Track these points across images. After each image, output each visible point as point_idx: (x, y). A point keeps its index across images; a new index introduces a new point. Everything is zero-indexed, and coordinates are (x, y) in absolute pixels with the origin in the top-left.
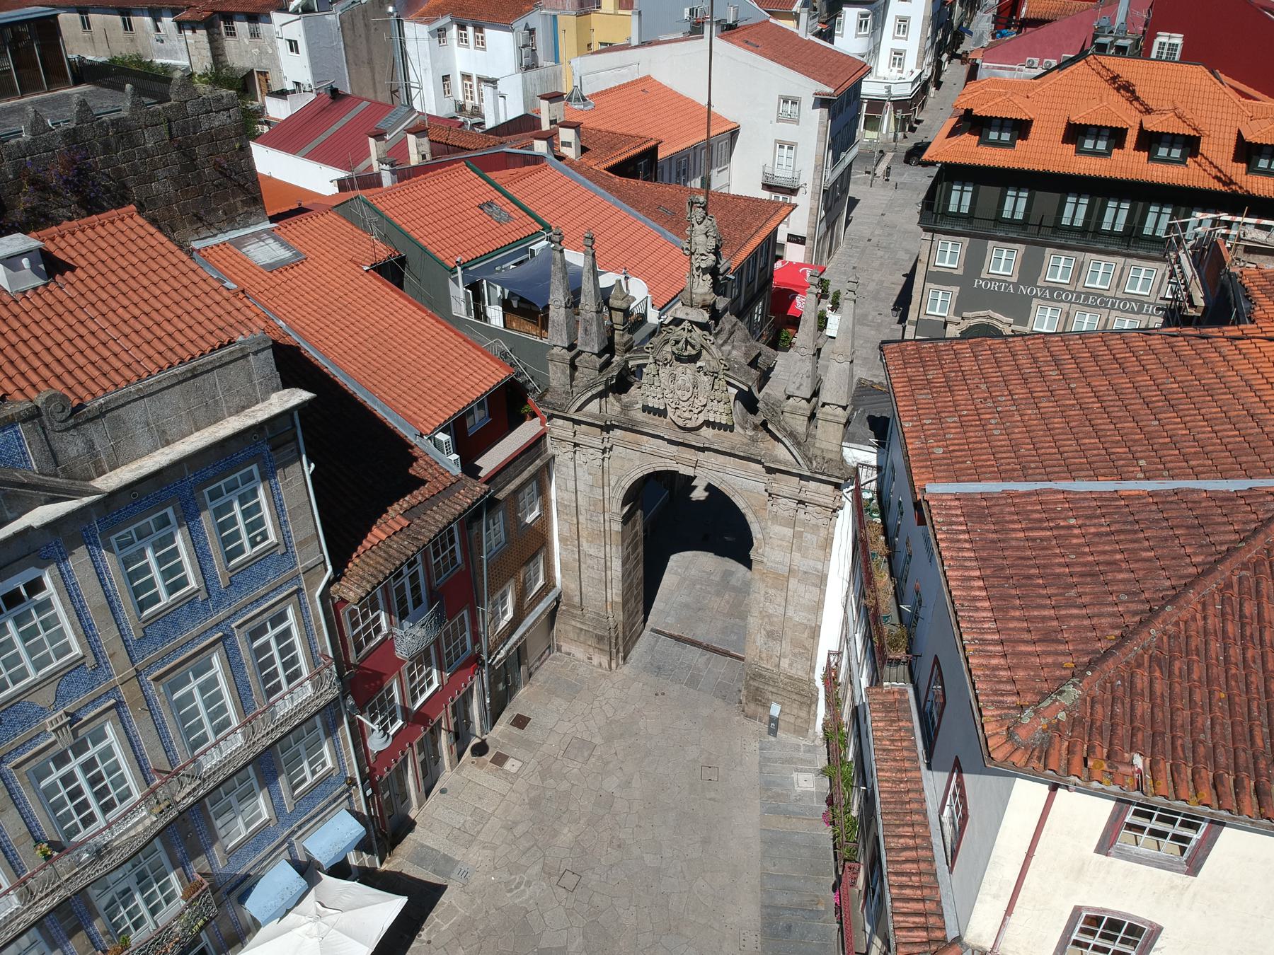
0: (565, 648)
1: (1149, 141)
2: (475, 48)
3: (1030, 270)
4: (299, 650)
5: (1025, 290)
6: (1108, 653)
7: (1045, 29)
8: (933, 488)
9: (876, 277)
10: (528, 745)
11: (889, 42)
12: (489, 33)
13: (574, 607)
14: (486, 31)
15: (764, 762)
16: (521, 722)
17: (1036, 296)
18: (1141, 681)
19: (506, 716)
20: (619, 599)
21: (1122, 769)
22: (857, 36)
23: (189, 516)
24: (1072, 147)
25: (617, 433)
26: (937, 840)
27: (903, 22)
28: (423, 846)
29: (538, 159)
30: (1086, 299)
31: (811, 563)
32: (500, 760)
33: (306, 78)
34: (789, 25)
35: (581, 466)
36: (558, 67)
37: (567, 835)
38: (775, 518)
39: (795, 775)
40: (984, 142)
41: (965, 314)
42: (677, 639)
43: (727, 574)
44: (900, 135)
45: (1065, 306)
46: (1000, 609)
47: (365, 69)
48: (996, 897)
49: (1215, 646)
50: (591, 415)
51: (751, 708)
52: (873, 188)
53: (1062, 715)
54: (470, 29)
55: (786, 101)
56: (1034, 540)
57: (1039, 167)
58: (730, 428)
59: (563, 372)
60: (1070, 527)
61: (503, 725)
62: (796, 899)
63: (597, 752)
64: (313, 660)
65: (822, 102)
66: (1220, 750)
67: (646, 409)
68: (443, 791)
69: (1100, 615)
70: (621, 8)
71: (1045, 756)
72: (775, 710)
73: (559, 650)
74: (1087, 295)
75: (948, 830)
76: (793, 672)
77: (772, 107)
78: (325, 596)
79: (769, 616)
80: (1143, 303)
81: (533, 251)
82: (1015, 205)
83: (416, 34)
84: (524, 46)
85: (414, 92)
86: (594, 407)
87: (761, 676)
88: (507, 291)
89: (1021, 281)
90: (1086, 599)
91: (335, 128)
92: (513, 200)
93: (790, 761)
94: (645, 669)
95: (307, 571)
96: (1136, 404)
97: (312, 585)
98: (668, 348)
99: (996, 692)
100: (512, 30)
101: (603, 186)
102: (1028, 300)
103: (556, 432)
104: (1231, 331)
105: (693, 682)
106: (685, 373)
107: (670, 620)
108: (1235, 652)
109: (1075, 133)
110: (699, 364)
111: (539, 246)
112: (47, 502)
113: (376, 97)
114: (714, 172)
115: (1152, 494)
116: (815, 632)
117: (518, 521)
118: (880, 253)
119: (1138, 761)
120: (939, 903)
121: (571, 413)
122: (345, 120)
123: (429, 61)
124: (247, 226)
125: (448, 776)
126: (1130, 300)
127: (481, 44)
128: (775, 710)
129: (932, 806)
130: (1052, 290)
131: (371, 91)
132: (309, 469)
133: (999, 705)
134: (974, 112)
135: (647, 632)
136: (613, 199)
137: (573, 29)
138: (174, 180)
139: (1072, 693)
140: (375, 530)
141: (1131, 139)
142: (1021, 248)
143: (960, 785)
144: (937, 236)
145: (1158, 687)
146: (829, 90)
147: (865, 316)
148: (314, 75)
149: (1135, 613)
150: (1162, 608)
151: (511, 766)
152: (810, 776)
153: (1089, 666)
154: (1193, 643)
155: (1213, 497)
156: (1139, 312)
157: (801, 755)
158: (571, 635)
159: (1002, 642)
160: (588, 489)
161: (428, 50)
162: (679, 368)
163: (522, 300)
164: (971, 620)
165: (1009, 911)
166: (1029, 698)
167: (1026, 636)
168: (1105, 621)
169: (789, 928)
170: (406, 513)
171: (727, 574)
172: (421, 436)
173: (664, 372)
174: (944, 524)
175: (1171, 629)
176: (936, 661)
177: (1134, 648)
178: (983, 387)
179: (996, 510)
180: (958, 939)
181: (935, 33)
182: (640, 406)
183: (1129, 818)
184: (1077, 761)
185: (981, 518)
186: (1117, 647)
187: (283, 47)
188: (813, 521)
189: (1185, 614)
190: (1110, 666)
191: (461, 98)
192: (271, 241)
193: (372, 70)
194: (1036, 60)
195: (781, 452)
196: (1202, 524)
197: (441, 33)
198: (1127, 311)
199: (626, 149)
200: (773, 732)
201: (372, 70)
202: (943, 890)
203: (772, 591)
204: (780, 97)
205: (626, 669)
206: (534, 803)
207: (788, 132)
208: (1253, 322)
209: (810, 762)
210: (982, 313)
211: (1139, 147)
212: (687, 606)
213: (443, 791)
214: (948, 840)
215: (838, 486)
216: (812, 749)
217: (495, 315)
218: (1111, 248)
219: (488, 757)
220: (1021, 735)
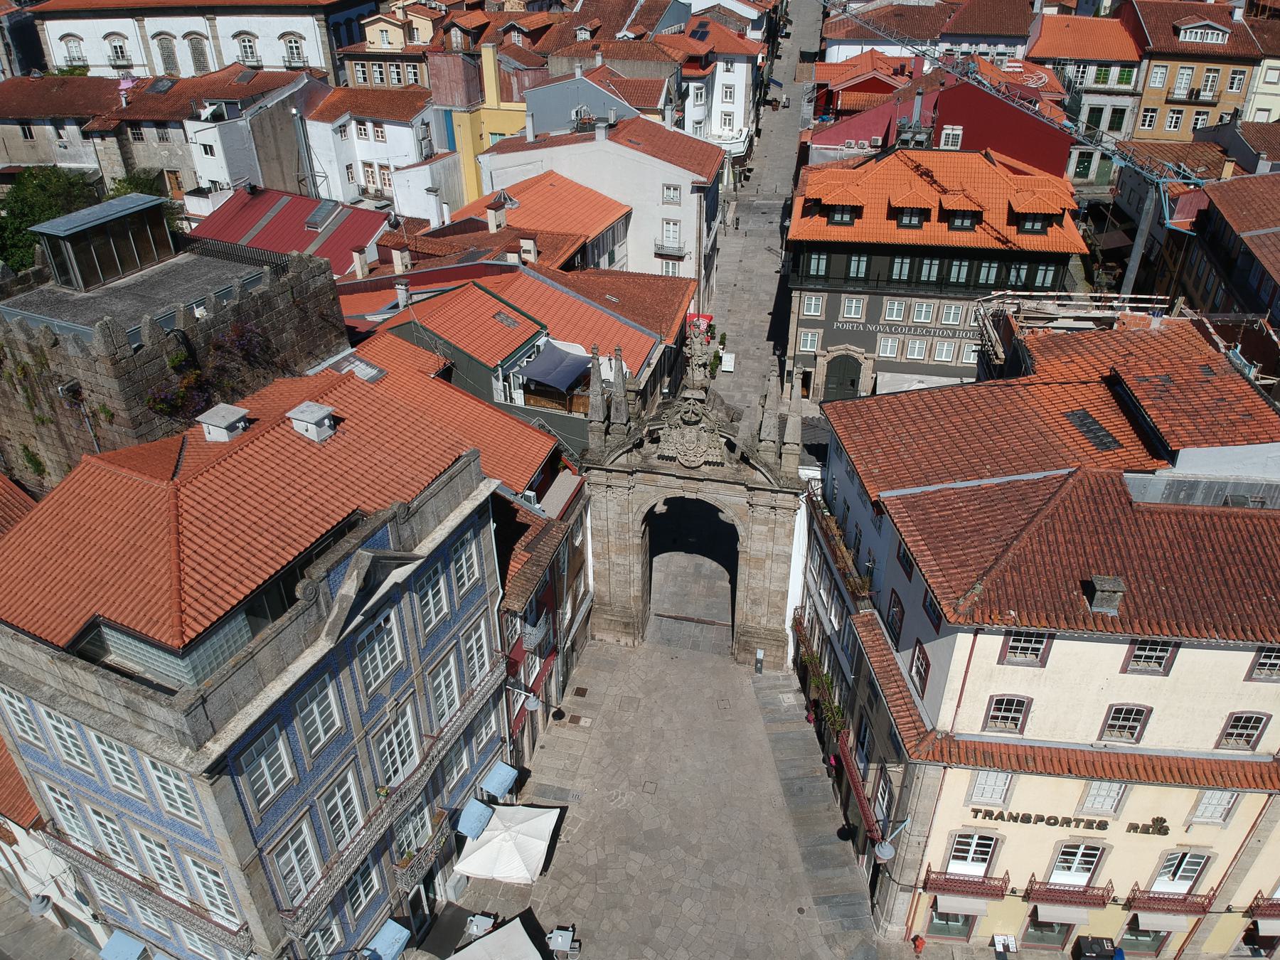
0: (598, 636)
1: (947, 216)
2: (376, 140)
3: (874, 313)
4: (485, 649)
5: (871, 328)
6: (991, 567)
7: (857, 118)
8: (884, 495)
9: (748, 317)
10: (592, 706)
11: (718, 106)
12: (388, 128)
13: (605, 605)
14: (386, 126)
15: (758, 691)
16: (581, 692)
17: (880, 331)
18: (1008, 579)
19: (569, 690)
20: (639, 594)
21: (1007, 617)
22: (695, 106)
23: (446, 567)
24: (894, 222)
25: (639, 475)
26: (911, 686)
27: (729, 91)
28: (541, 785)
29: (512, 269)
30: (915, 331)
31: (781, 548)
32: (575, 720)
33: (223, 177)
34: (655, 119)
35: (611, 501)
36: (456, 156)
37: (639, 759)
38: (754, 520)
39: (780, 696)
40: (831, 222)
41: (829, 348)
42: (676, 618)
43: (698, 567)
44: (739, 185)
45: (901, 337)
46: (936, 554)
47: (275, 165)
48: (951, 699)
49: (1038, 557)
50: (621, 465)
51: (742, 656)
52: (728, 238)
53: (976, 598)
54: (369, 126)
55: (668, 188)
56: (944, 516)
57: (874, 240)
58: (722, 465)
59: (600, 438)
60: (961, 507)
61: (569, 698)
62: (801, 772)
63: (643, 703)
64: (491, 656)
65: (697, 189)
66: (1047, 603)
67: (661, 457)
68: (542, 747)
69: (984, 550)
70: (503, 100)
71: (972, 617)
72: (760, 654)
73: (593, 638)
74: (916, 328)
75: (916, 679)
76: (770, 626)
77: (658, 192)
78: (499, 610)
79: (753, 589)
80: (955, 330)
81: (538, 346)
82: (858, 266)
83: (319, 133)
84: (423, 139)
85: (319, 180)
86: (623, 459)
87: (748, 632)
88: (525, 378)
89: (868, 321)
90: (976, 544)
91: (263, 222)
92: (515, 309)
93: (775, 687)
94: (658, 642)
95: (492, 593)
96: (979, 432)
97: (493, 604)
98: (678, 416)
99: (944, 593)
100: (412, 127)
101: (560, 283)
102: (874, 334)
103: (593, 479)
104: (1023, 380)
105: (695, 646)
106: (691, 432)
107: (666, 606)
108: (1047, 559)
109: (895, 213)
110: (701, 425)
111: (541, 341)
112: (396, 568)
113: (286, 187)
114: (616, 247)
115: (997, 485)
116: (784, 595)
117: (573, 544)
118: (746, 296)
119: (1012, 613)
120: (919, 715)
121: (607, 466)
122: (271, 215)
123: (334, 154)
124: (338, 353)
125: (542, 737)
126: (946, 329)
127: (380, 137)
128: (760, 654)
129: (904, 671)
130: (891, 326)
131: (281, 183)
132: (493, 526)
133: (947, 599)
134: (823, 202)
135: (652, 617)
136: (582, 298)
137: (468, 125)
138: (296, 329)
139: (979, 588)
140: (512, 563)
141: (935, 214)
142: (866, 297)
143: (922, 651)
144: (804, 293)
145: (1016, 579)
146: (703, 179)
147: (747, 351)
148: (231, 175)
149: (1000, 547)
150: (1012, 543)
151: (584, 722)
152: (790, 695)
153: (984, 574)
154: (1029, 557)
155: (1028, 483)
156: (954, 337)
157: (781, 682)
158: (603, 626)
159: (941, 570)
160: (617, 516)
161: (333, 146)
162: (688, 429)
163: (538, 383)
164: (924, 562)
165: (958, 706)
166: (960, 593)
167: (952, 566)
168: (987, 553)
169: (801, 789)
170: (528, 548)
171: (698, 567)
172: (517, 494)
173: (675, 433)
174: (895, 513)
175: (1018, 552)
176: (893, 591)
177: (1003, 563)
178: (891, 428)
179: (920, 503)
180: (934, 729)
181: (754, 95)
182: (656, 455)
183: (1011, 644)
184: (986, 617)
185: (914, 508)
186: (995, 564)
187: (197, 151)
188: (781, 519)
189: (1023, 544)
190: (993, 573)
191: (363, 183)
192: (357, 363)
193: (281, 164)
194: (853, 142)
195: (759, 476)
196: (1023, 499)
197: (342, 129)
198: (945, 337)
199: (565, 248)
200: (759, 670)
201: (281, 164)
202: (920, 709)
203: (754, 571)
204: (664, 185)
205: (645, 645)
206: (609, 744)
207: (672, 212)
208: (1035, 373)
209: (789, 686)
210: (841, 347)
211: (940, 220)
212: (675, 594)
213: (542, 747)
214: (918, 684)
215: (796, 495)
216: (787, 678)
217: (519, 397)
218: (930, 294)
219: (566, 719)
220: (961, 609)
